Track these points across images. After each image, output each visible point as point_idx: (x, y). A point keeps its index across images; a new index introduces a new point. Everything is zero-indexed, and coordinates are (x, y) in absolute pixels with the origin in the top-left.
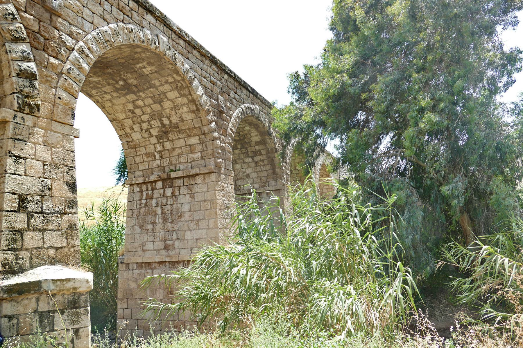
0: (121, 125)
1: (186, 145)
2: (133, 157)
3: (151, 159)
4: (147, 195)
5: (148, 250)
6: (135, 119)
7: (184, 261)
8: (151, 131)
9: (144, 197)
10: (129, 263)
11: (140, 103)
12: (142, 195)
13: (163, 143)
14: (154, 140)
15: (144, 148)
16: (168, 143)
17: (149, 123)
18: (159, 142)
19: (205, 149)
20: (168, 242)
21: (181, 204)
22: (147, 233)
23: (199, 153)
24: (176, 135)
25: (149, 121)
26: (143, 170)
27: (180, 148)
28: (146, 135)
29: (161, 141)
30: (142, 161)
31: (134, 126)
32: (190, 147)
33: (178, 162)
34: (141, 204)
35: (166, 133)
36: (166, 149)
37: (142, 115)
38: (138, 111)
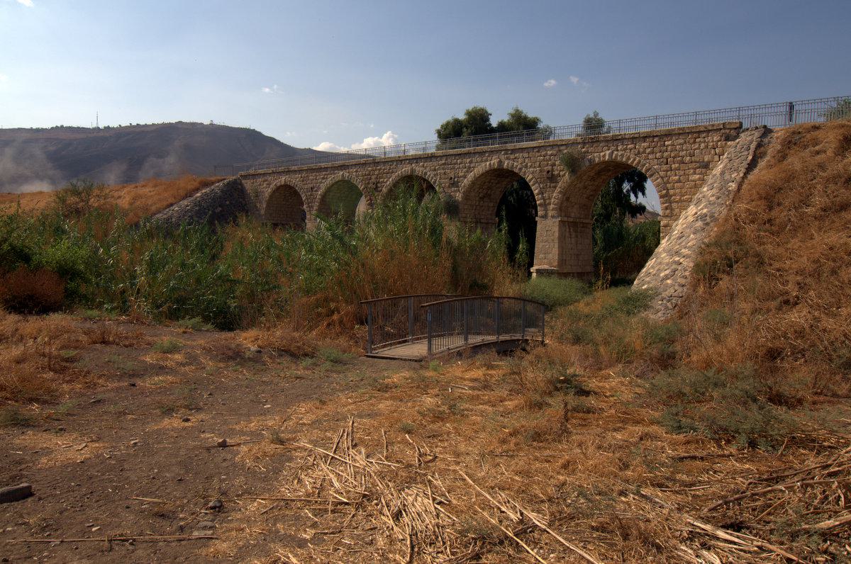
14: (477, 199)
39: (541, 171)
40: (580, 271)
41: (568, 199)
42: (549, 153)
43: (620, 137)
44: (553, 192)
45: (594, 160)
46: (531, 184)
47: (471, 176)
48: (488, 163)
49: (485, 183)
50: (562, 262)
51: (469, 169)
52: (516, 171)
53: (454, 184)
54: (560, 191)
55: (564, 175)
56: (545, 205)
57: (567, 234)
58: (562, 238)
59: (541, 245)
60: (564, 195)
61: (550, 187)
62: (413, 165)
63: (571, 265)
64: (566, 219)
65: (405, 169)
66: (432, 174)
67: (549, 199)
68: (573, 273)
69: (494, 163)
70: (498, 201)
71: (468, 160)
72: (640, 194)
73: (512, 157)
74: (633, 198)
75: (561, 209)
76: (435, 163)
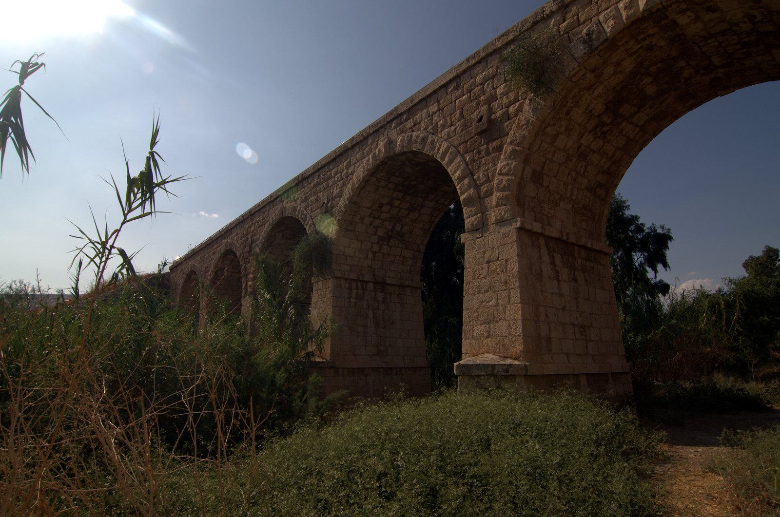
1: (401, 255)
7: (397, 368)
9: (354, 295)
10: (338, 368)
11: (397, 203)
14: (374, 239)
16: (386, 247)
17: (383, 222)
19: (414, 265)
23: (409, 267)
24: (397, 243)
27: (395, 256)
32: (404, 259)
33: (388, 269)
36: (382, 252)
38: (386, 208)
39: (465, 127)
40: (594, 369)
41: (538, 177)
42: (479, 78)
47: (348, 191)
49: (381, 206)
50: (537, 342)
54: (514, 151)
55: (520, 110)
56: (479, 200)
57: (547, 270)
58: (530, 277)
60: (526, 161)
63: (568, 355)
64: (537, 227)
67: (488, 180)
68: (576, 376)
70: (423, 248)
72: (660, 267)
73: (409, 124)
74: (650, 274)
75: (519, 201)
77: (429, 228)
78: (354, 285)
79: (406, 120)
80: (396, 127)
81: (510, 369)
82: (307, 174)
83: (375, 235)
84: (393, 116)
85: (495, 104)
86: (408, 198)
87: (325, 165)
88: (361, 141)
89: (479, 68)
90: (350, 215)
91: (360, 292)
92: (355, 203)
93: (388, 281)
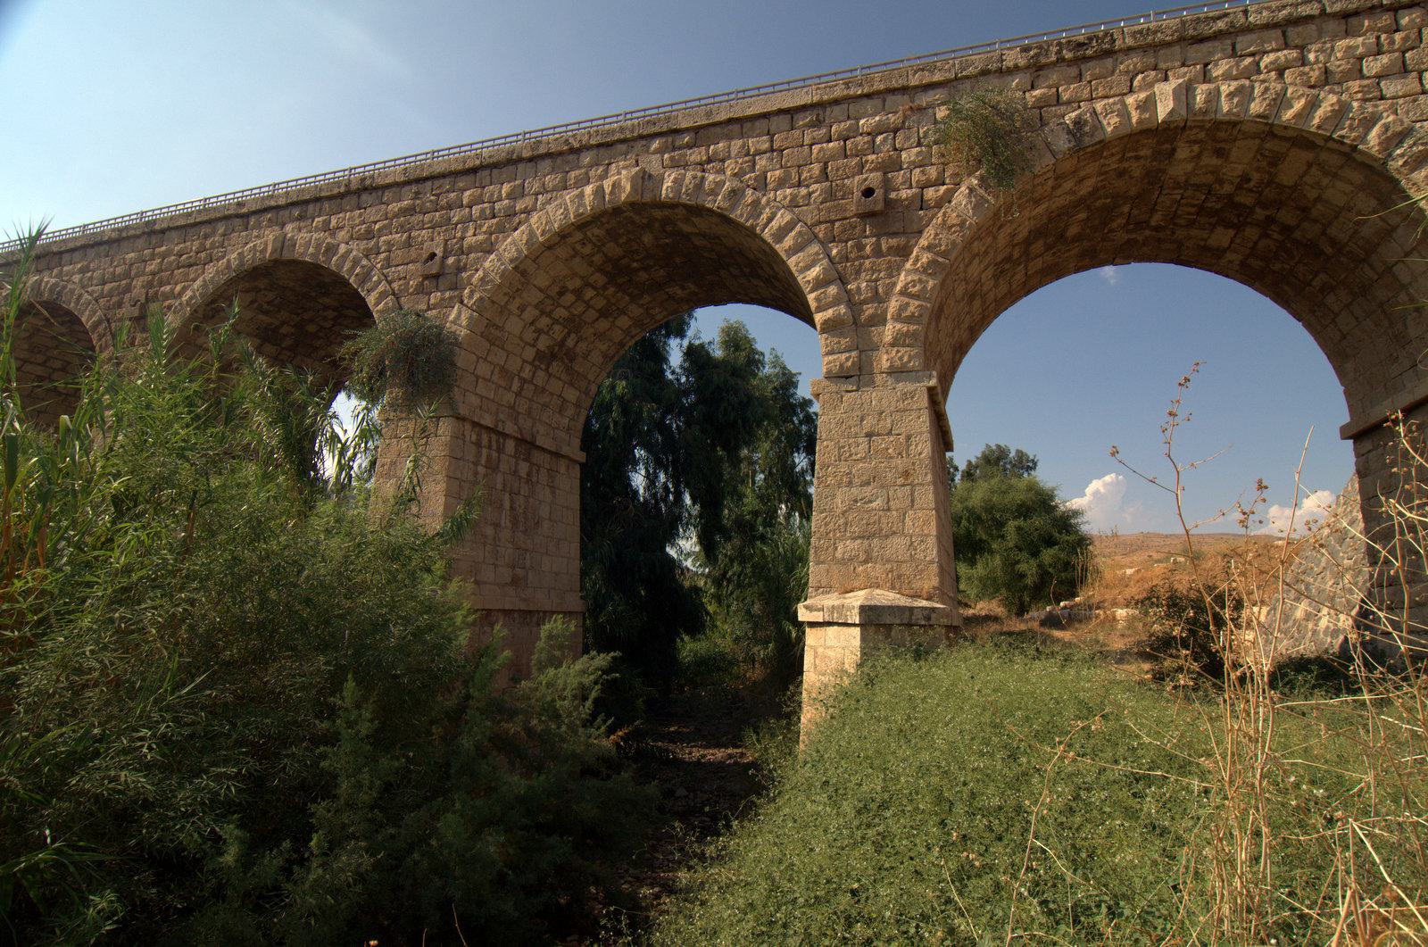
0: (518, 290)
2: (478, 358)
3: (503, 383)
4: (489, 457)
5: (486, 583)
6: (548, 302)
7: (538, 612)
8: (543, 337)
11: (589, 293)
12: (479, 455)
13: (537, 368)
14: (529, 353)
15: (505, 355)
18: (532, 363)
20: (519, 572)
21: (540, 502)
22: (485, 544)
25: (556, 321)
26: (482, 397)
27: (552, 394)
28: (529, 336)
29: (537, 363)
30: (488, 377)
31: (529, 309)
34: (476, 473)
35: (553, 356)
37: (564, 307)
38: (569, 298)
39: (830, 195)
43: (1221, 25)
44: (893, 270)
45: (1098, 126)
46: (780, 248)
47: (513, 244)
48: (589, 190)
51: (510, 220)
52: (718, 202)
53: (441, 276)
54: (932, 263)
59: (840, 502)
61: (877, 252)
62: (289, 227)
65: (260, 243)
66: (357, 248)
67: (878, 298)
69: (616, 185)
71: (506, 188)
73: (696, 155)
76: (372, 213)
77: (613, 356)
78: (485, 437)
79: (689, 146)
80: (661, 151)
81: (933, 616)
82: (380, 181)
83: (534, 346)
84: (656, 129)
85: (899, 177)
86: (611, 290)
87: (443, 176)
88: (561, 154)
89: (869, 105)
90: (505, 294)
91: (495, 454)
92: (524, 273)
93: (540, 442)
